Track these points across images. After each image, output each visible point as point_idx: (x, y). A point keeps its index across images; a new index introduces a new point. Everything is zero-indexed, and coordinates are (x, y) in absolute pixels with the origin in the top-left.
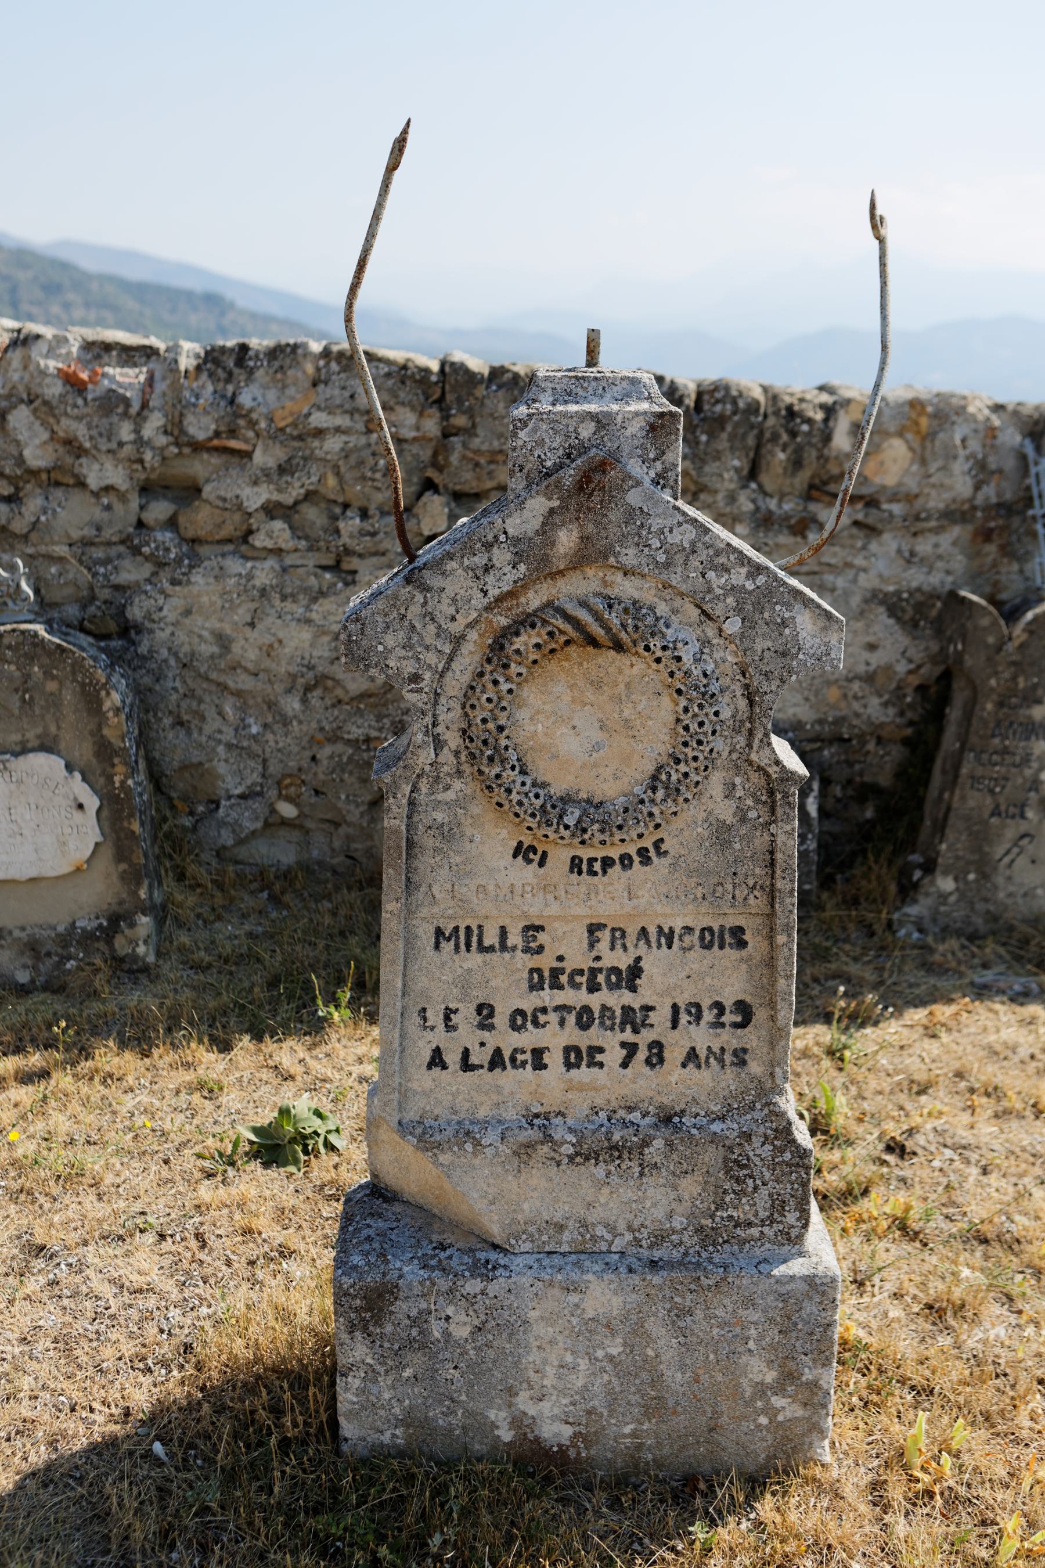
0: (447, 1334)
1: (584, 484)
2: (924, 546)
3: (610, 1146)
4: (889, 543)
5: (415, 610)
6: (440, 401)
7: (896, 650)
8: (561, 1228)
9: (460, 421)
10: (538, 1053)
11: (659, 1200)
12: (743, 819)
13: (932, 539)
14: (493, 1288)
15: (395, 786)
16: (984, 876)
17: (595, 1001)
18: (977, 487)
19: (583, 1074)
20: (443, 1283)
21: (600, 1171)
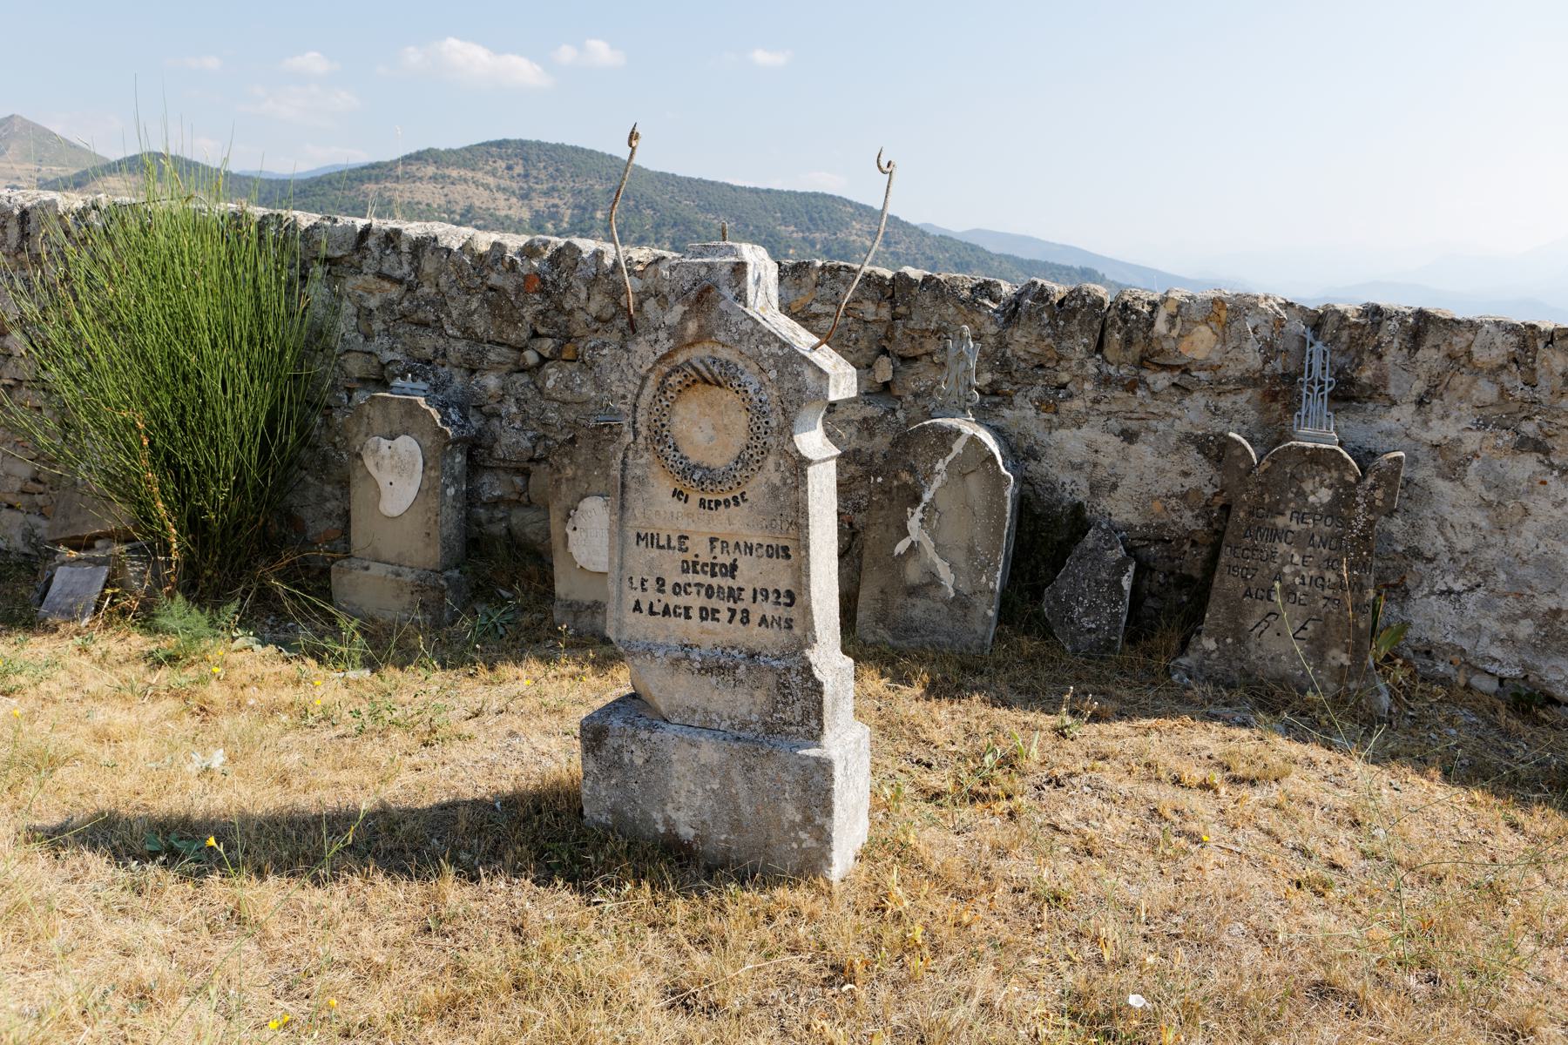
0: (631, 761)
1: (699, 299)
2: (1225, 403)
3: (717, 668)
4: (1198, 400)
5: (624, 362)
6: (893, 296)
7: (1202, 476)
8: (695, 711)
9: (902, 310)
10: (687, 609)
11: (742, 702)
12: (785, 484)
13: (1232, 398)
14: (654, 737)
15: (614, 455)
16: (1239, 641)
17: (715, 582)
18: (1266, 362)
19: (709, 624)
20: (630, 730)
21: (714, 680)
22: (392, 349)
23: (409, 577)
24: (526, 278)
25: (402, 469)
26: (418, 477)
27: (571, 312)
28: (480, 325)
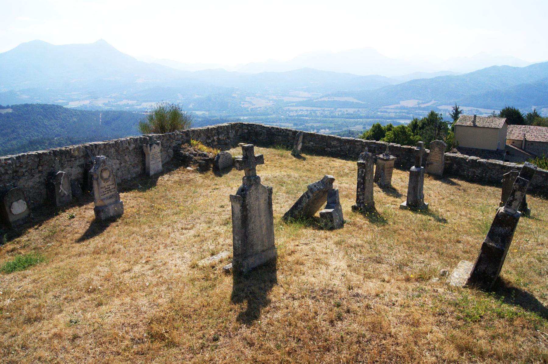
3: (111, 197)
4: (78, 160)
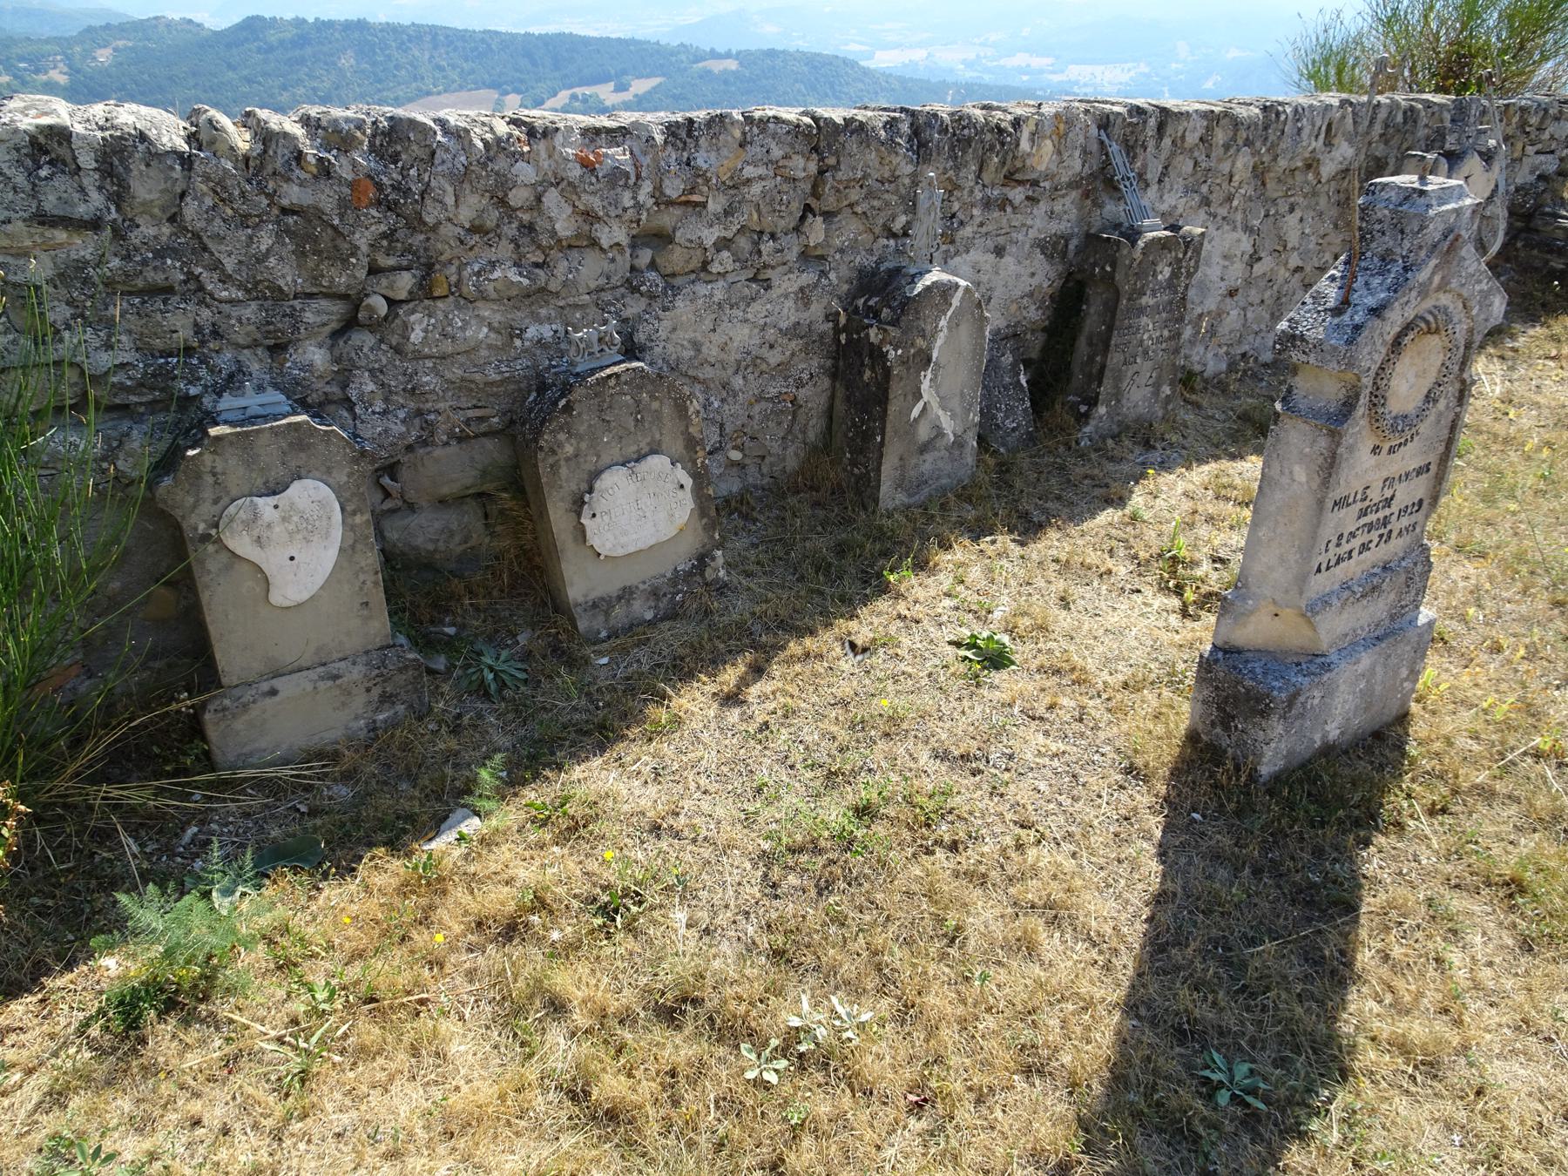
4: (1043, 206)
9: (832, 161)
16: (1118, 401)
22: (108, 346)
23: (356, 673)
24: (352, 185)
25: (307, 530)
26: (337, 533)
27: (435, 228)
28: (287, 275)
